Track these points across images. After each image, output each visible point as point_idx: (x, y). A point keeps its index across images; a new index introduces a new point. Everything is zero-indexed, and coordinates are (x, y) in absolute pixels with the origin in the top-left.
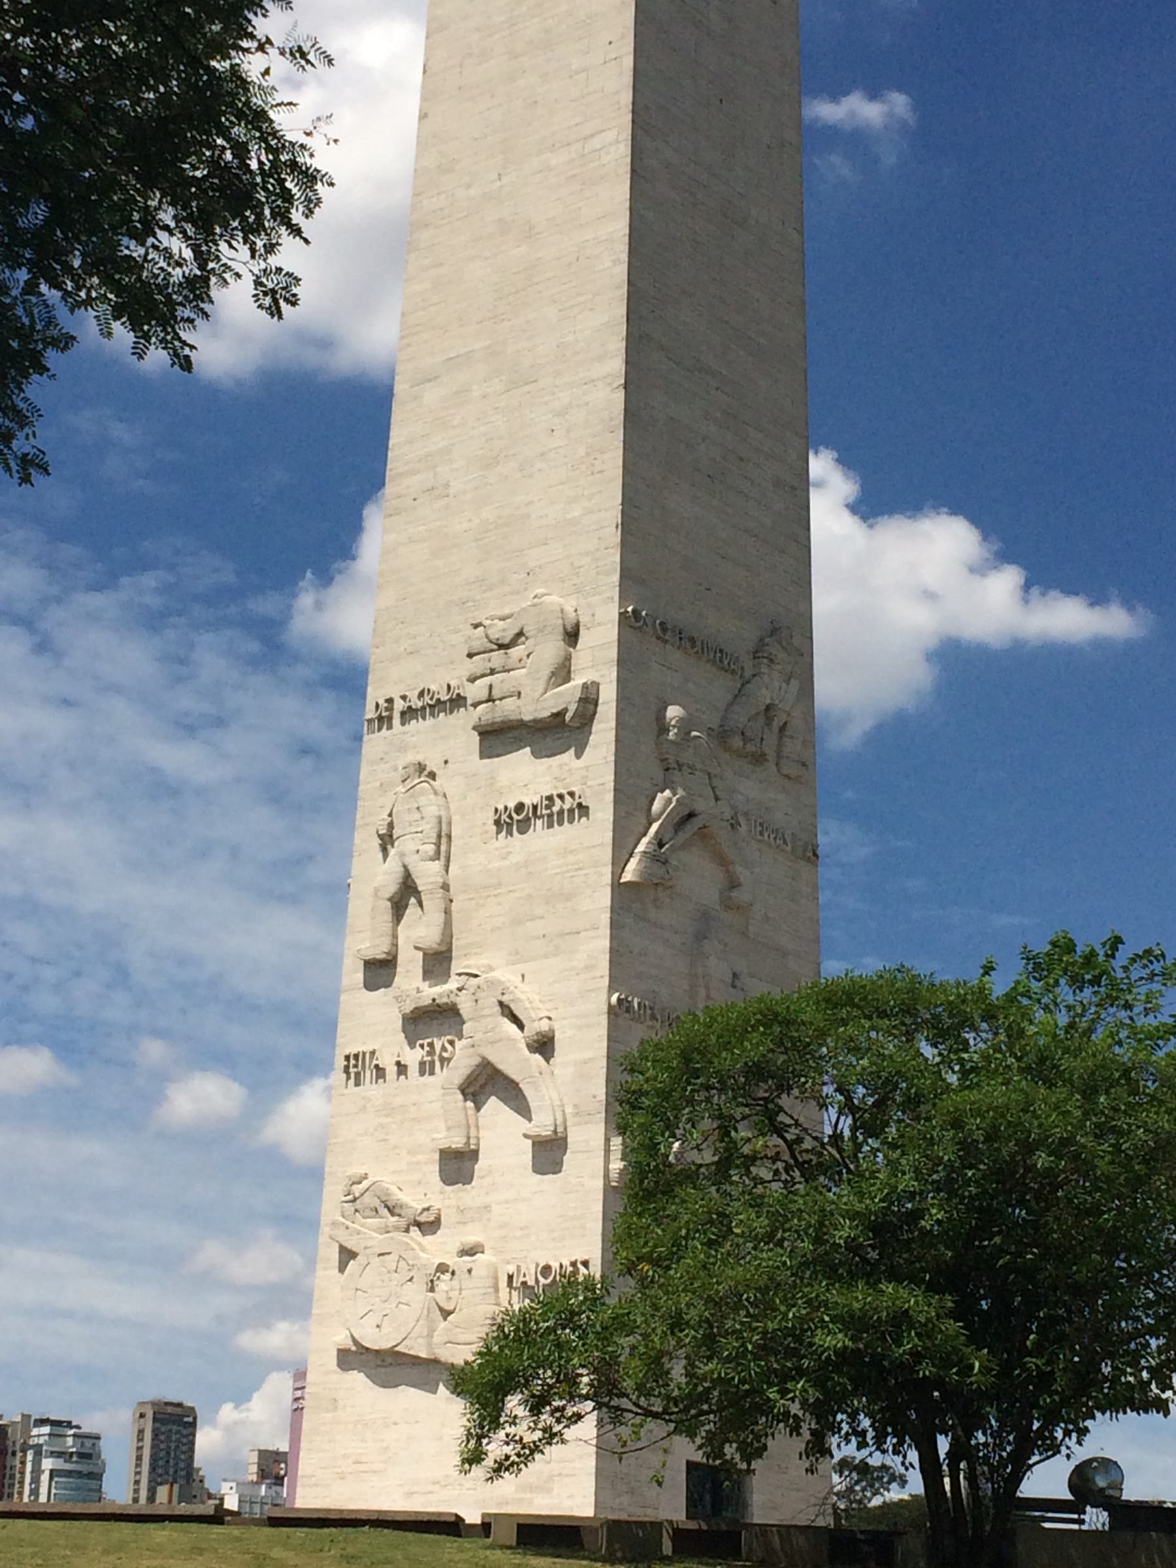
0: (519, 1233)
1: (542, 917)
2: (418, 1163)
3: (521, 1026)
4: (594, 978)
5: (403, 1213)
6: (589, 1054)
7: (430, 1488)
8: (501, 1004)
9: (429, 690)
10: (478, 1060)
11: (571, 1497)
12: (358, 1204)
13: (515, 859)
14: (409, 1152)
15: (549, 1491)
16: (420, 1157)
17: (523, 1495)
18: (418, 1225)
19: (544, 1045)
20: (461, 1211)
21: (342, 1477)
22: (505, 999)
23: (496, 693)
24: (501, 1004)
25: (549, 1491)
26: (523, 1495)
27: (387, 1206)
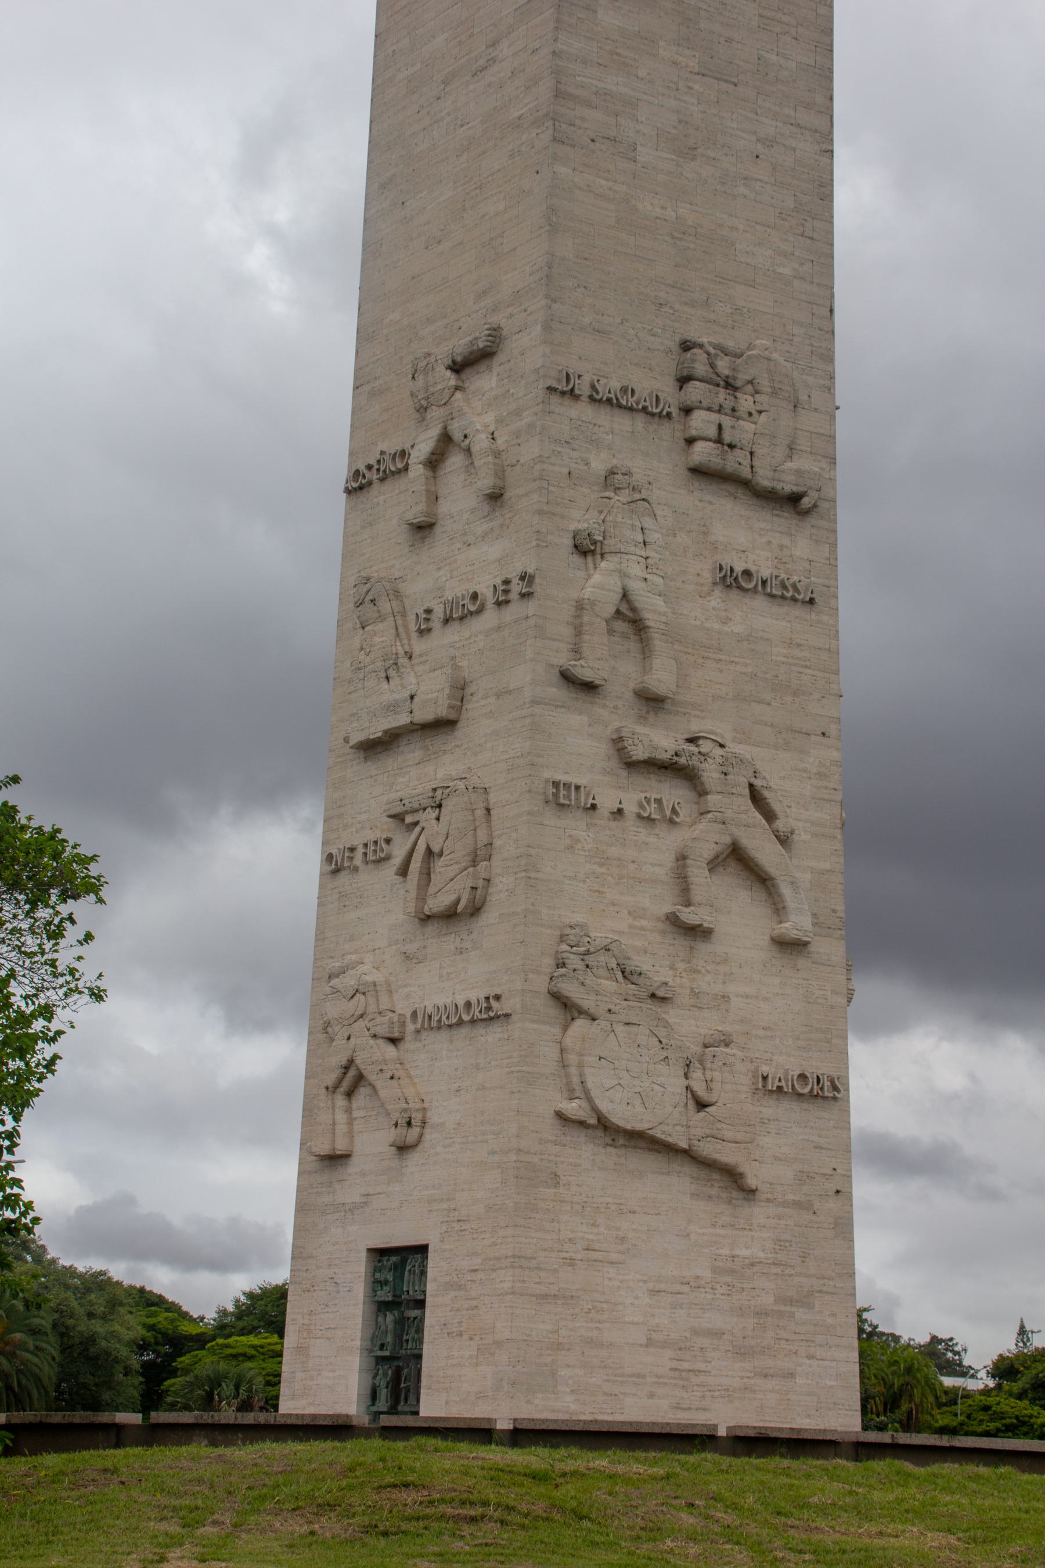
0: (761, 1033)
1: (769, 704)
2: (643, 928)
3: (769, 815)
4: (826, 788)
5: (641, 981)
6: (827, 866)
7: (678, 1287)
8: (751, 786)
9: (633, 391)
10: (728, 840)
11: (833, 1315)
12: (590, 960)
13: (737, 627)
14: (630, 913)
15: (810, 1306)
16: (644, 923)
17: (782, 1308)
18: (653, 996)
19: (784, 840)
20: (695, 994)
21: (571, 1262)
22: (758, 783)
23: (727, 438)
24: (751, 786)
25: (810, 1306)
26: (782, 1308)
27: (623, 972)
